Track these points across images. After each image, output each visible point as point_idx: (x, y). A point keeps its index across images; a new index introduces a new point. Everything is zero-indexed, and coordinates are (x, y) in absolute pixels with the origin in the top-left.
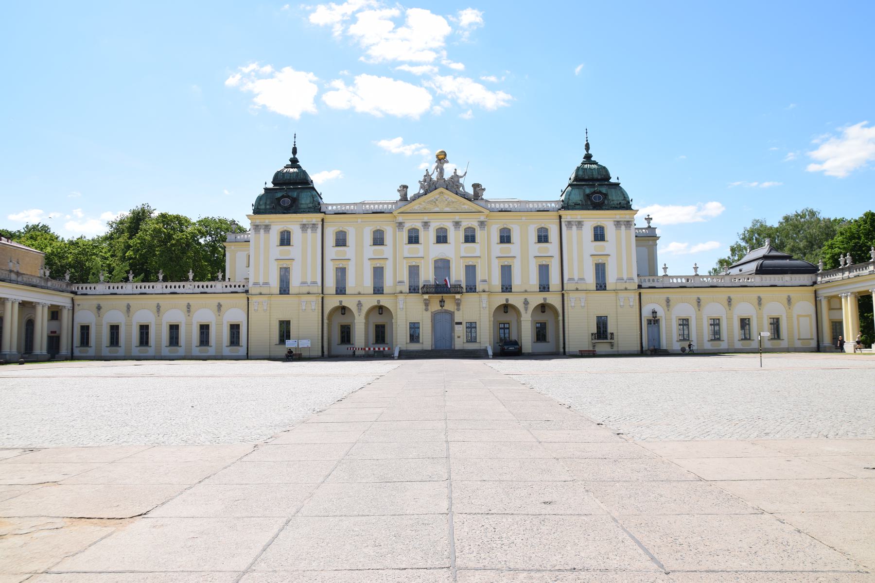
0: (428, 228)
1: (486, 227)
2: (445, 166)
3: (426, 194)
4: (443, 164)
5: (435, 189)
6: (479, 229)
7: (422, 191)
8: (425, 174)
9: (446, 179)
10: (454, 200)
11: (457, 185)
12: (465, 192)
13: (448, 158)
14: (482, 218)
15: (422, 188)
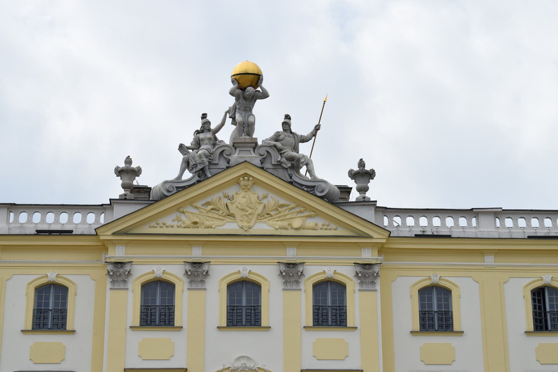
0: (202, 282)
1: (378, 282)
2: (259, 106)
3: (199, 182)
4: (254, 98)
5: (228, 168)
6: (357, 287)
7: (187, 175)
8: (199, 129)
9: (260, 143)
10: (282, 201)
11: (291, 159)
12: (315, 180)
13: (266, 84)
14: (368, 256)
15: (188, 163)
